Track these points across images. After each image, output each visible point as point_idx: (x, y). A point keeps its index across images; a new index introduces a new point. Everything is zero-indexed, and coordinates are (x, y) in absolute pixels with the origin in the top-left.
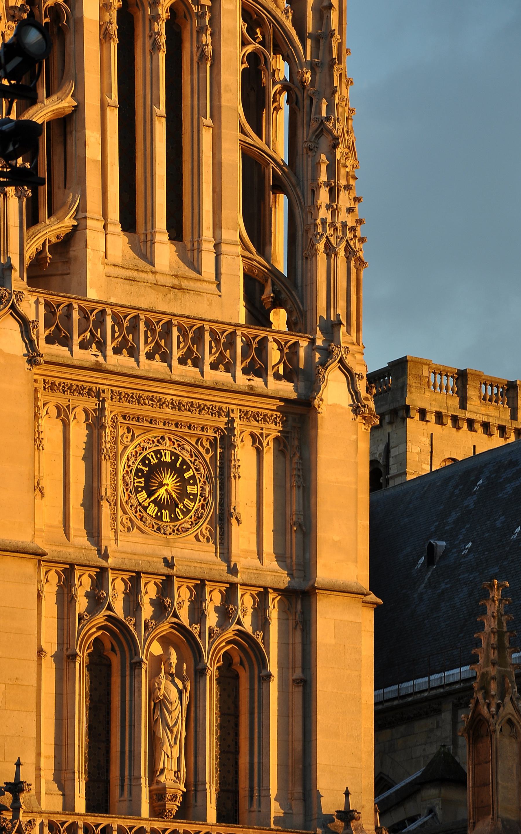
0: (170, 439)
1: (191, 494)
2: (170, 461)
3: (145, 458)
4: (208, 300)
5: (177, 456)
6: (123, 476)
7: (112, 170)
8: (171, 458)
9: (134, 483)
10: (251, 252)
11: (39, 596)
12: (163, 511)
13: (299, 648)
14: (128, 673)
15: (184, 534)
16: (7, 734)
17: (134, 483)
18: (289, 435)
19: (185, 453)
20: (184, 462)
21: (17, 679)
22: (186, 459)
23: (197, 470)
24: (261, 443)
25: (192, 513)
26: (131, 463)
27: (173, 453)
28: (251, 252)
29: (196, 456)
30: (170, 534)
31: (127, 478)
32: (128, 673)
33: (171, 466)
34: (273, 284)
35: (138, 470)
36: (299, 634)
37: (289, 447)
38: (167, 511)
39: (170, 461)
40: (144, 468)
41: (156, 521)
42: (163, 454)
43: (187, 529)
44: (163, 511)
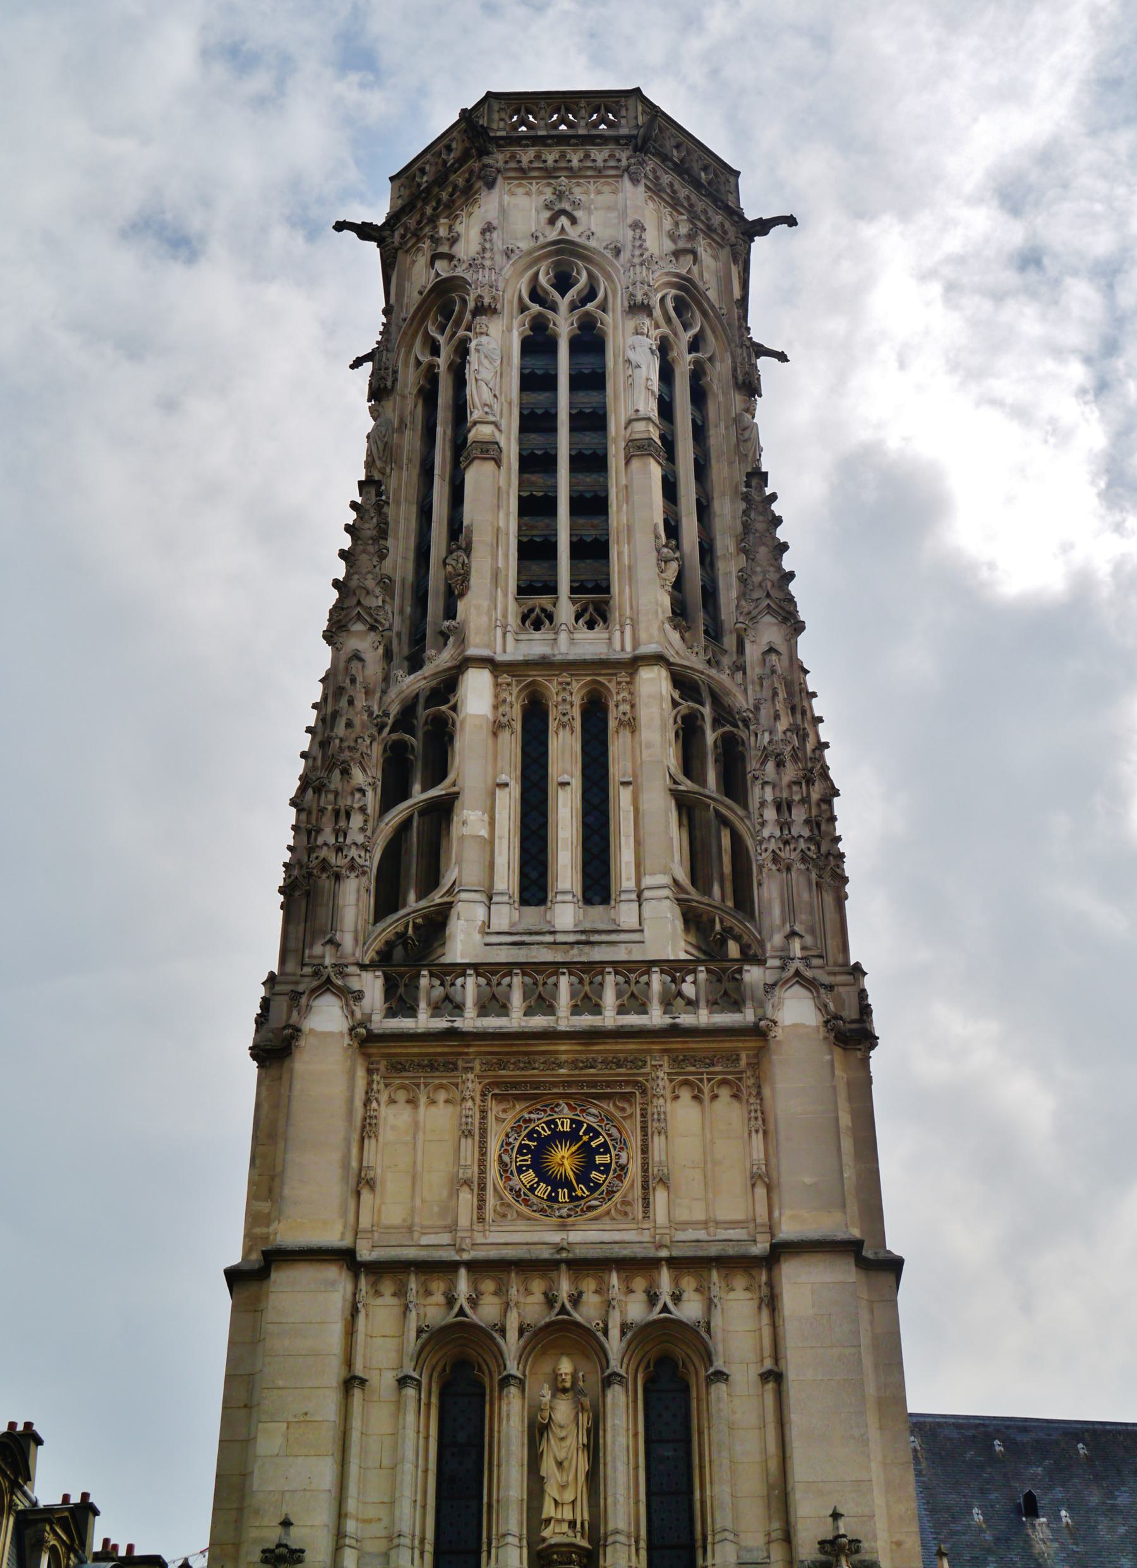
0: (567, 1104)
1: (601, 1165)
2: (568, 1130)
3: (533, 1131)
4: (626, 949)
5: (580, 1124)
6: (500, 1156)
7: (500, 843)
8: (571, 1127)
9: (516, 1162)
10: (688, 893)
11: (354, 1311)
12: (560, 1190)
13: (766, 1331)
14: (496, 1394)
15: (591, 1214)
16: (286, 1489)
17: (516, 1162)
18: (744, 1075)
19: (591, 1119)
20: (590, 1129)
21: (306, 1414)
22: (595, 1125)
23: (610, 1135)
24: (700, 1090)
25: (604, 1188)
26: (511, 1140)
27: (572, 1121)
28: (688, 893)
29: (608, 1119)
30: (569, 1216)
31: (506, 1158)
32: (496, 1394)
33: (572, 1137)
34: (721, 922)
35: (522, 1146)
36: (765, 1312)
37: (744, 1090)
38: (565, 1190)
39: (568, 1130)
40: (531, 1143)
41: (549, 1203)
42: (559, 1123)
43: (595, 1208)
44: (560, 1190)
